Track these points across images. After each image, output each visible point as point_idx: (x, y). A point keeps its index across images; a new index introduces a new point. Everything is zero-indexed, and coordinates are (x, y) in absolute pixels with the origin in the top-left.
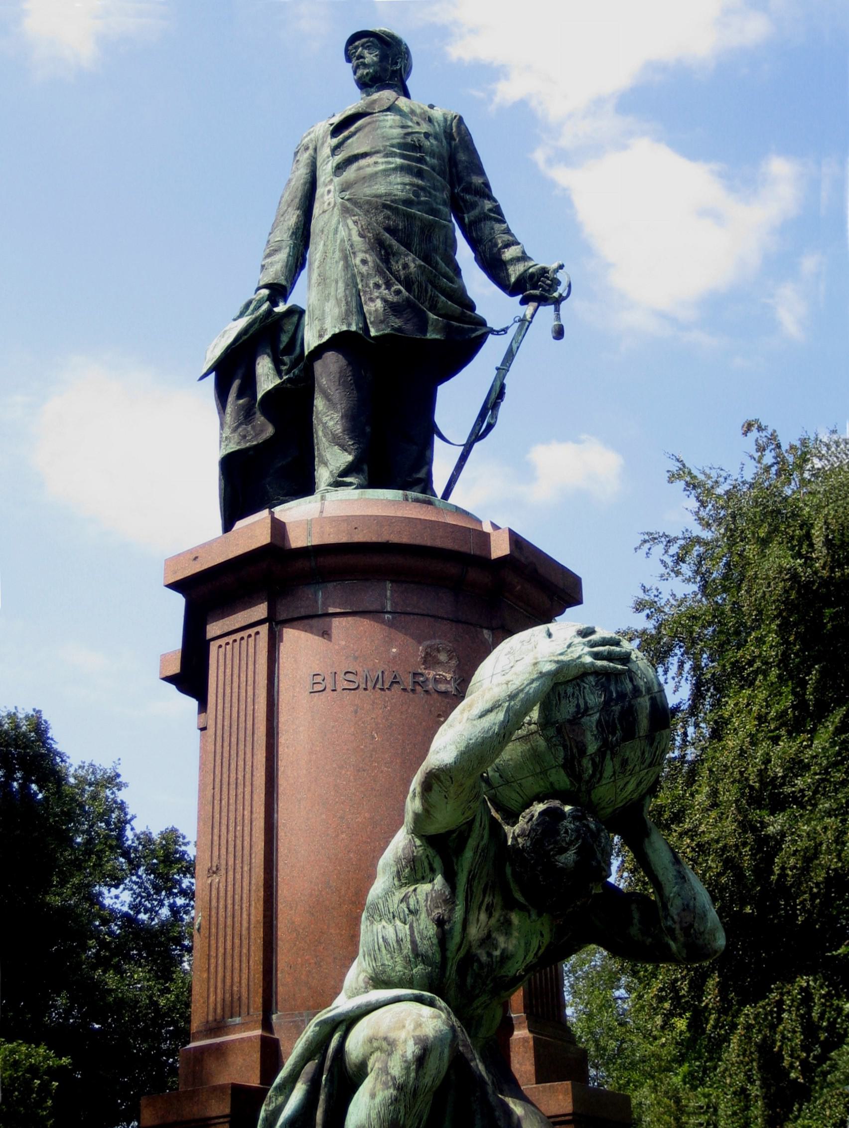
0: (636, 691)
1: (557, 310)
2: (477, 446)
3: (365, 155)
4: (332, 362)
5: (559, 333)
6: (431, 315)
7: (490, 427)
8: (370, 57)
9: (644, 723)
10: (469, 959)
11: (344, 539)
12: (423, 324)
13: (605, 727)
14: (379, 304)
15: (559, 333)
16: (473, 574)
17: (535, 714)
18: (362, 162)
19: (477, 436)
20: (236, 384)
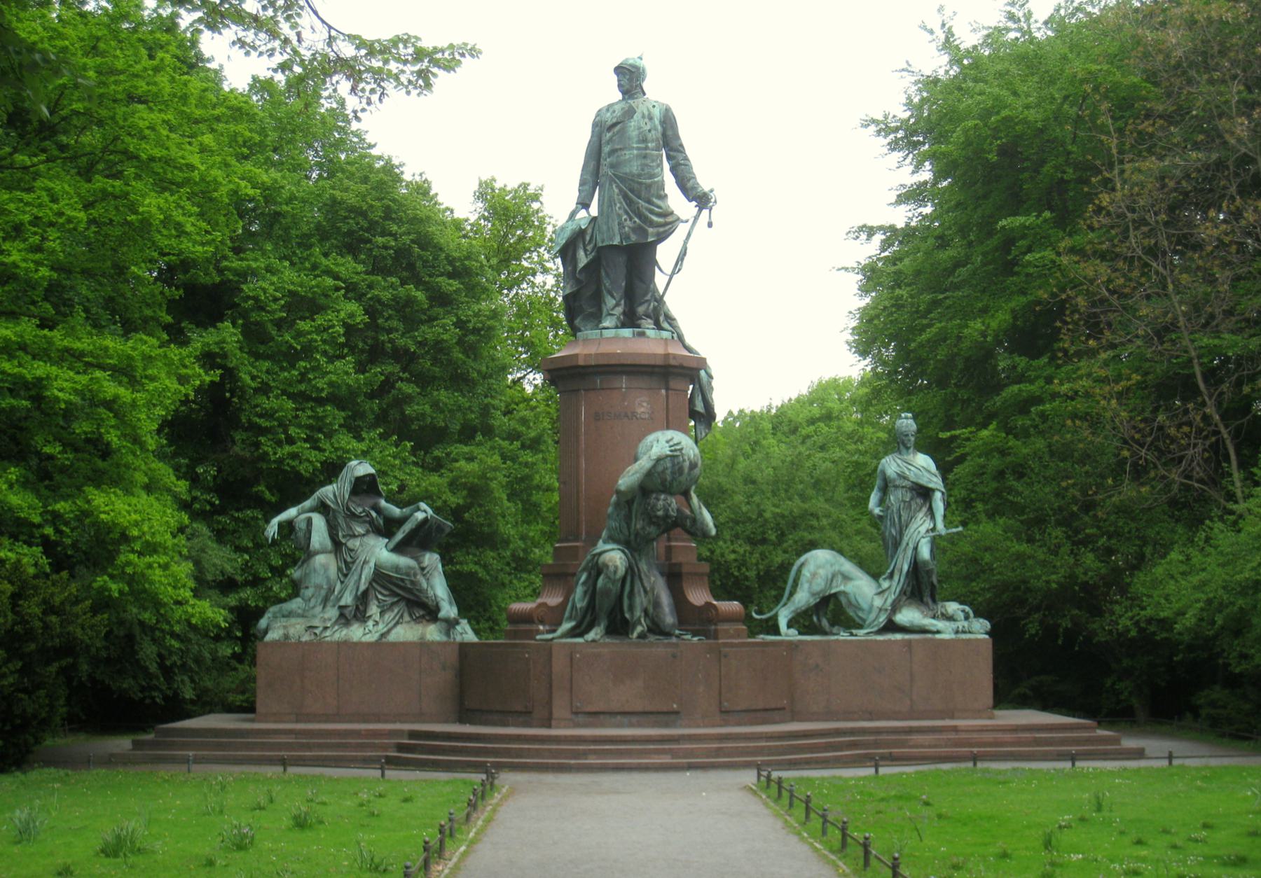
0: (684, 460)
2: (675, 276)
3: (621, 149)
5: (710, 225)
6: (650, 230)
8: (625, 82)
9: (686, 470)
10: (637, 535)
12: (646, 233)
13: (673, 473)
14: (627, 229)
15: (710, 225)
16: (656, 370)
18: (619, 153)
19: (673, 273)
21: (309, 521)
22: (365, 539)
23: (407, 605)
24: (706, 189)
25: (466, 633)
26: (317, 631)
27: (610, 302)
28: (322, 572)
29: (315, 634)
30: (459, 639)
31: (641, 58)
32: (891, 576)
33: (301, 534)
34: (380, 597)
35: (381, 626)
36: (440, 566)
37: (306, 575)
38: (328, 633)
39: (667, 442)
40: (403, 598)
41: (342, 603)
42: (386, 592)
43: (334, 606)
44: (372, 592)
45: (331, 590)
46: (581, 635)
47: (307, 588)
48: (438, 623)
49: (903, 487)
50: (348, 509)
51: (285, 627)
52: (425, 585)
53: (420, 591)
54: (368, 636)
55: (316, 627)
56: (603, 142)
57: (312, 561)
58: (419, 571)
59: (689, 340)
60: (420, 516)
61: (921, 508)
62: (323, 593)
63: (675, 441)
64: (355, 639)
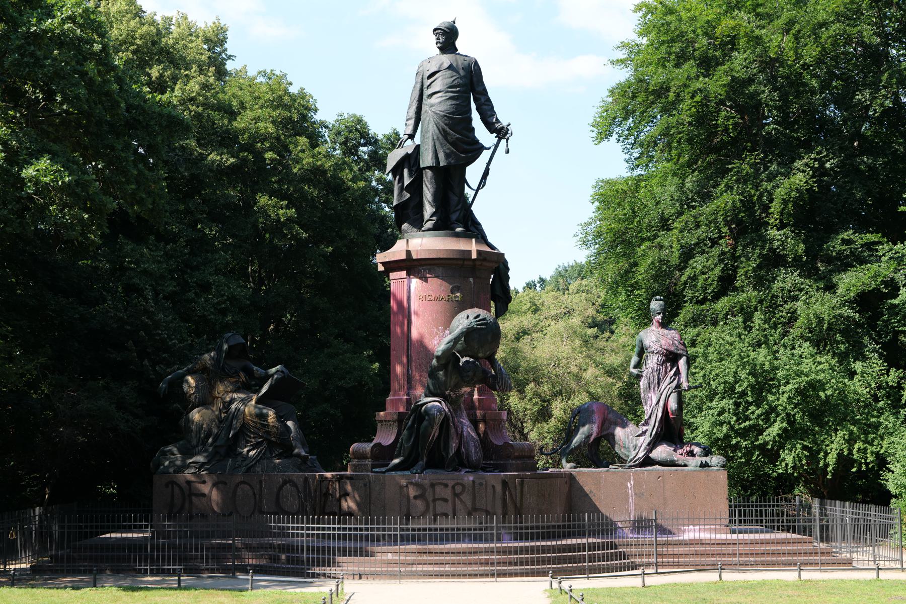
1: (507, 142)
4: (429, 173)
5: (508, 152)
7: (483, 186)
8: (442, 39)
11: (427, 257)
15: (508, 152)
17: (463, 339)
19: (478, 188)
20: (398, 177)
24: (505, 124)
27: (428, 210)
31: (454, 23)
32: (647, 423)
39: (475, 318)
46: (407, 469)
49: (657, 353)
56: (425, 86)
59: (490, 239)
61: (671, 370)
63: (481, 317)
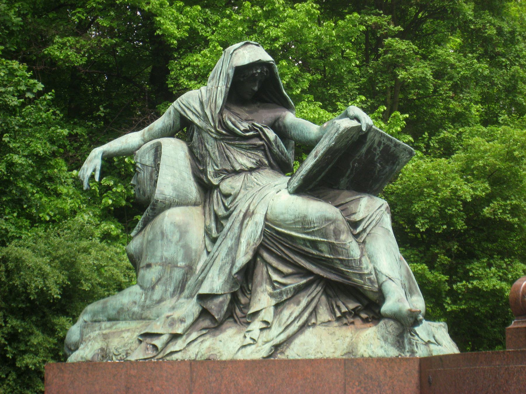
21: (157, 151)
22: (254, 177)
23: (325, 292)
25: (438, 343)
26: (159, 342)
28: (176, 237)
29: (155, 347)
30: (421, 352)
33: (144, 175)
34: (275, 277)
35: (275, 330)
36: (387, 220)
37: (150, 243)
38: (179, 345)
40: (318, 279)
41: (205, 290)
42: (286, 269)
43: (191, 296)
44: (261, 270)
45: (190, 269)
47: (149, 266)
48: (382, 323)
50: (223, 124)
51: (105, 337)
52: (355, 251)
53: (347, 263)
54: (249, 349)
55: (158, 335)
57: (161, 216)
58: (344, 226)
60: (345, 124)
62: (177, 274)
64: (226, 356)
